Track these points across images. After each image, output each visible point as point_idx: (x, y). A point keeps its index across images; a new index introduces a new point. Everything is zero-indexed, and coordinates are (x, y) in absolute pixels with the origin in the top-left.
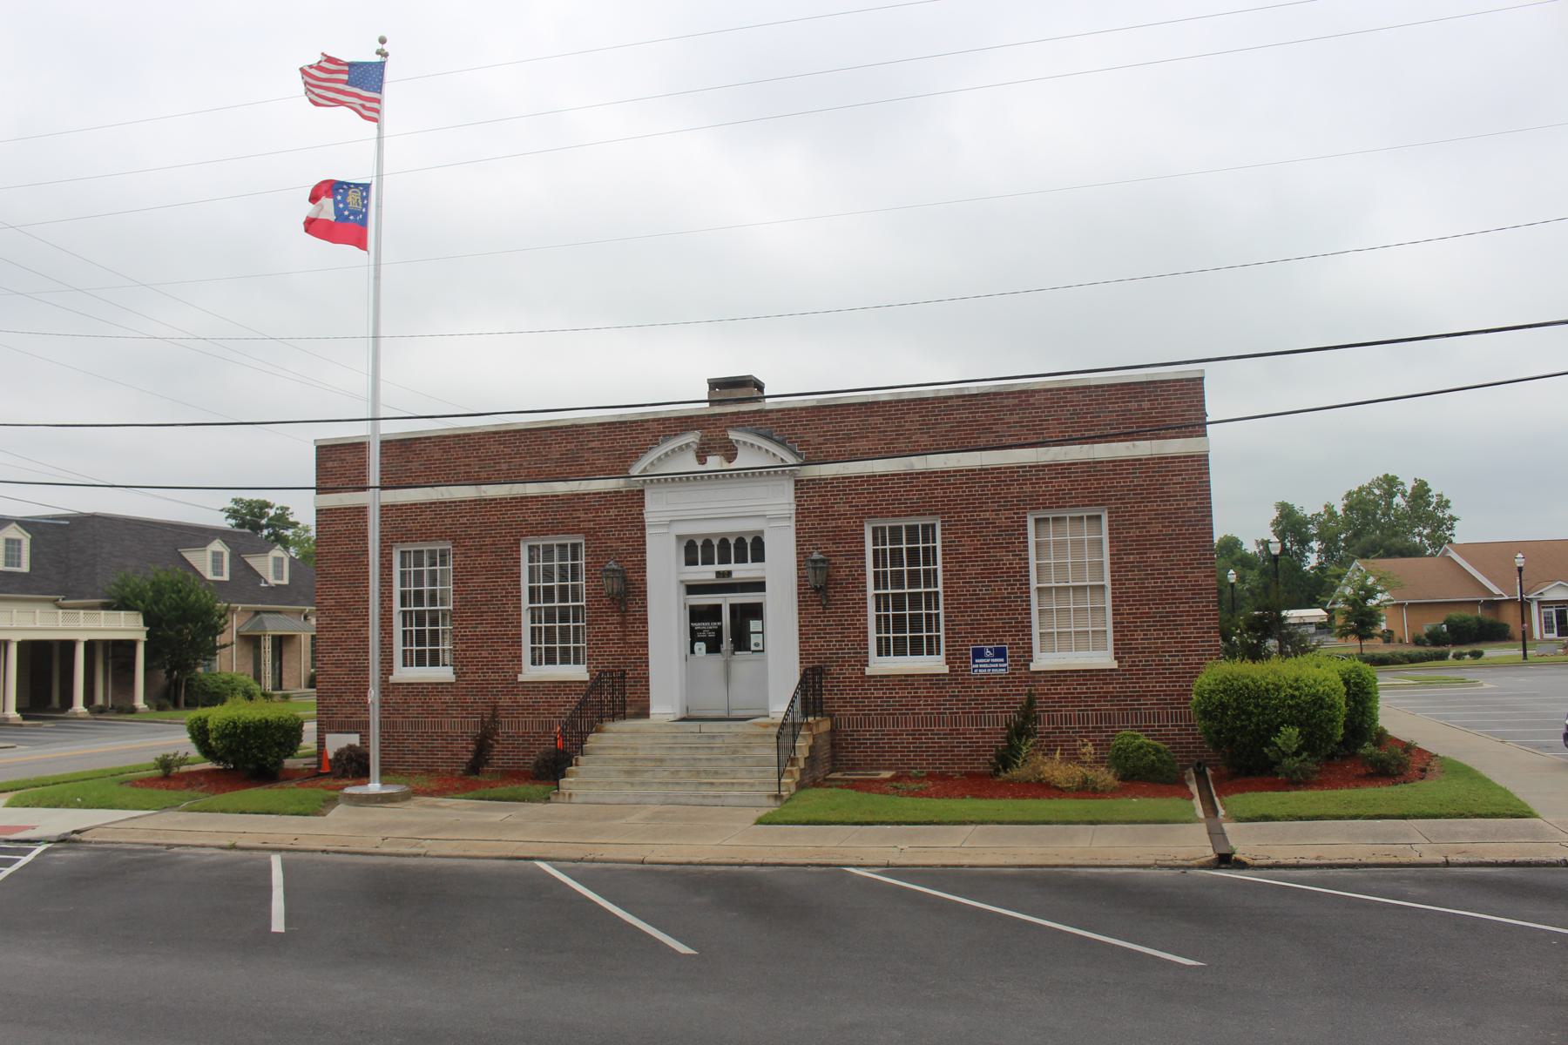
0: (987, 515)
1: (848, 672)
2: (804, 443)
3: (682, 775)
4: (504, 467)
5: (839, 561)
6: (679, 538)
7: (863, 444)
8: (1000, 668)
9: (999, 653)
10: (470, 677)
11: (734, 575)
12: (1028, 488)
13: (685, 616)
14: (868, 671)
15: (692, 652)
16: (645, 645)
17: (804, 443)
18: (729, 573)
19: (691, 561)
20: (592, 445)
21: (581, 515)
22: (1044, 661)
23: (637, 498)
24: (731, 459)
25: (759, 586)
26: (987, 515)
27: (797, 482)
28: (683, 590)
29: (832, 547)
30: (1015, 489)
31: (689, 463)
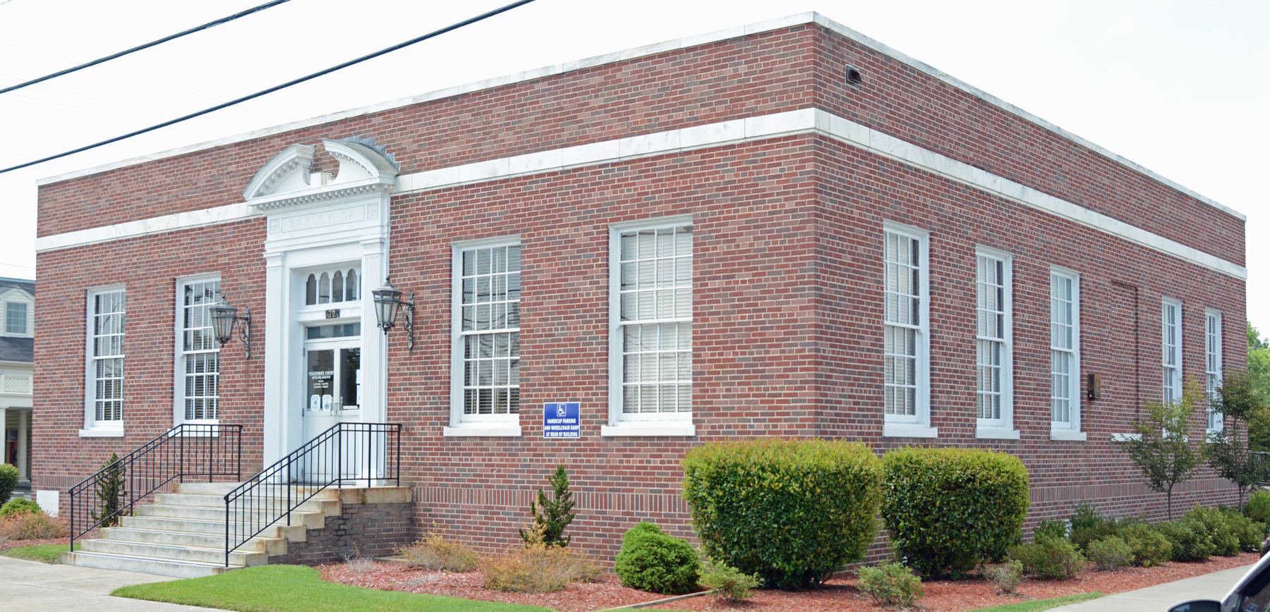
0: (566, 231)
1: (429, 432)
2: (401, 151)
3: (181, 540)
4: (165, 198)
5: (425, 294)
6: (296, 271)
7: (453, 149)
8: (570, 432)
9: (572, 413)
10: (135, 431)
11: (342, 315)
12: (609, 194)
13: (302, 363)
14: (447, 432)
15: (309, 406)
16: (261, 396)
17: (401, 151)
18: (337, 312)
19: (310, 300)
20: (231, 168)
21: (218, 248)
22: (622, 425)
23: (255, 228)
24: (335, 174)
25: (350, 329)
26: (566, 231)
27: (393, 199)
28: (302, 333)
29: (420, 279)
30: (596, 196)
31: (297, 186)
